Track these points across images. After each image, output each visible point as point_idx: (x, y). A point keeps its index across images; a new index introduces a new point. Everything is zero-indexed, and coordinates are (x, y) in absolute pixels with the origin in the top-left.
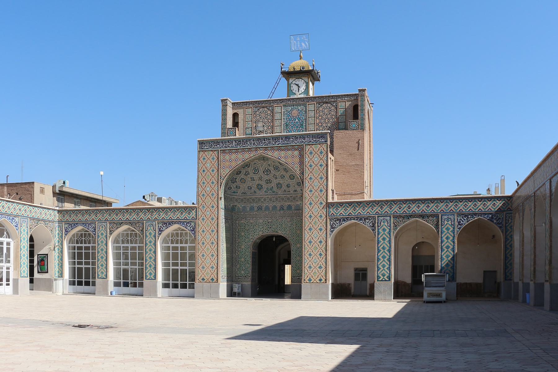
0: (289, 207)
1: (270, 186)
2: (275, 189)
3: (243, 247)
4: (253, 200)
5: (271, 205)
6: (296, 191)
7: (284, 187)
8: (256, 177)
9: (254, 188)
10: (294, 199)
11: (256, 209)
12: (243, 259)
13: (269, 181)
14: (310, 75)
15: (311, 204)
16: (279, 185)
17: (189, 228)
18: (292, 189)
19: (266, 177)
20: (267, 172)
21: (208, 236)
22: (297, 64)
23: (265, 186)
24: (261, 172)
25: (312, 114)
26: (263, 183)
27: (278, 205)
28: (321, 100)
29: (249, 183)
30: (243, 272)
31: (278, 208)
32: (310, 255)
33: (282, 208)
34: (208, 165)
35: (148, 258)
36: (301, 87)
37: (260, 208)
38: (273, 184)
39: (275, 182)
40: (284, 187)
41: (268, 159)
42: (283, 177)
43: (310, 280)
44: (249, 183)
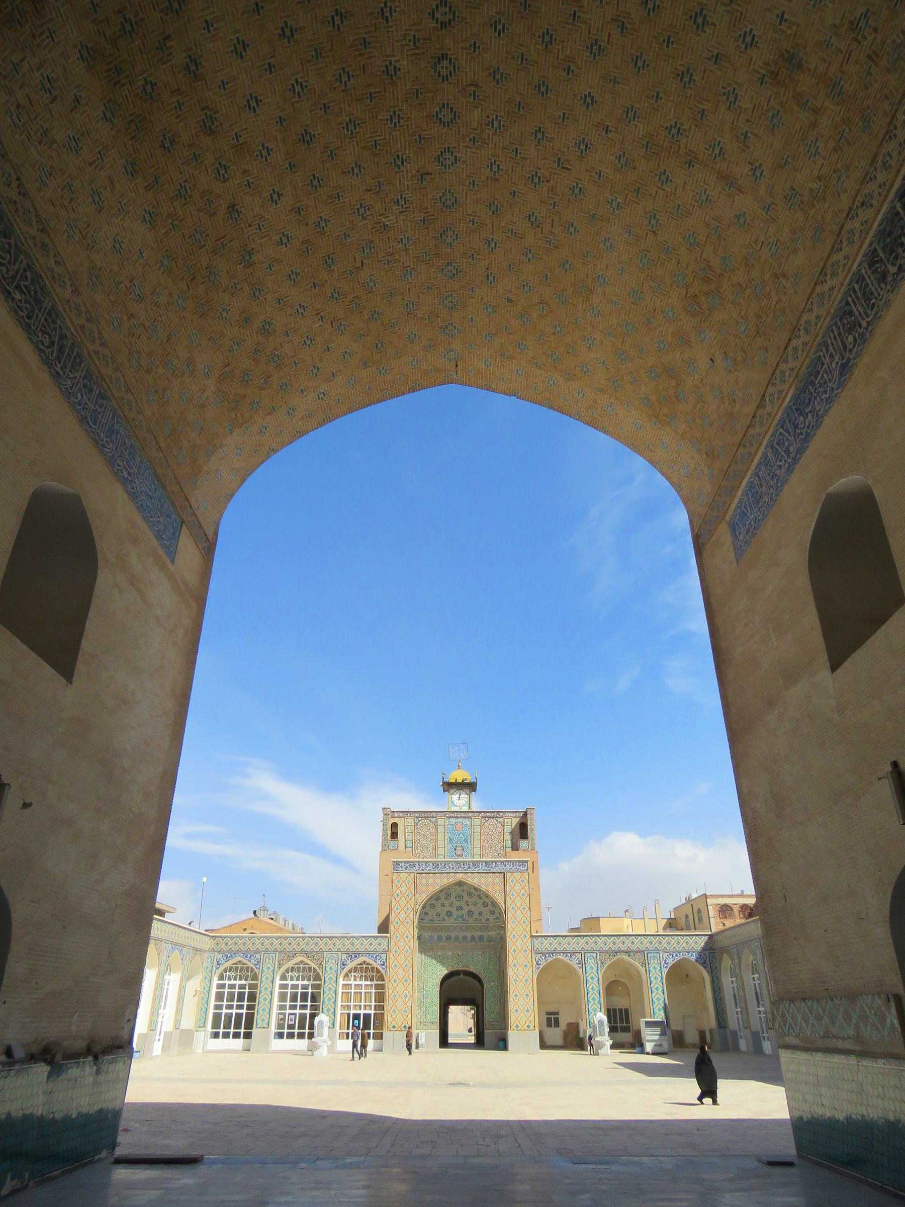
0: (481, 938)
1: (460, 913)
2: (465, 917)
3: (429, 984)
4: (442, 929)
5: (461, 935)
6: (488, 920)
7: (476, 915)
8: (447, 903)
9: (443, 915)
10: (486, 928)
11: (444, 939)
12: (429, 1000)
13: (459, 908)
14: (470, 787)
15: (514, 936)
16: (470, 913)
17: (378, 962)
18: (484, 917)
19: (461, 903)
20: (460, 897)
21: (401, 972)
22: (458, 775)
23: (455, 913)
24: (453, 898)
25: (477, 829)
26: (453, 910)
27: (469, 935)
28: (488, 815)
29: (439, 909)
30: (429, 1017)
31: (469, 939)
32: (516, 995)
33: (473, 939)
34: (403, 889)
35: (325, 1000)
36: (459, 801)
37: (448, 938)
38: (465, 912)
39: (466, 909)
40: (476, 915)
41: (467, 884)
42: (475, 904)
43: (517, 1026)
44: (439, 909)
